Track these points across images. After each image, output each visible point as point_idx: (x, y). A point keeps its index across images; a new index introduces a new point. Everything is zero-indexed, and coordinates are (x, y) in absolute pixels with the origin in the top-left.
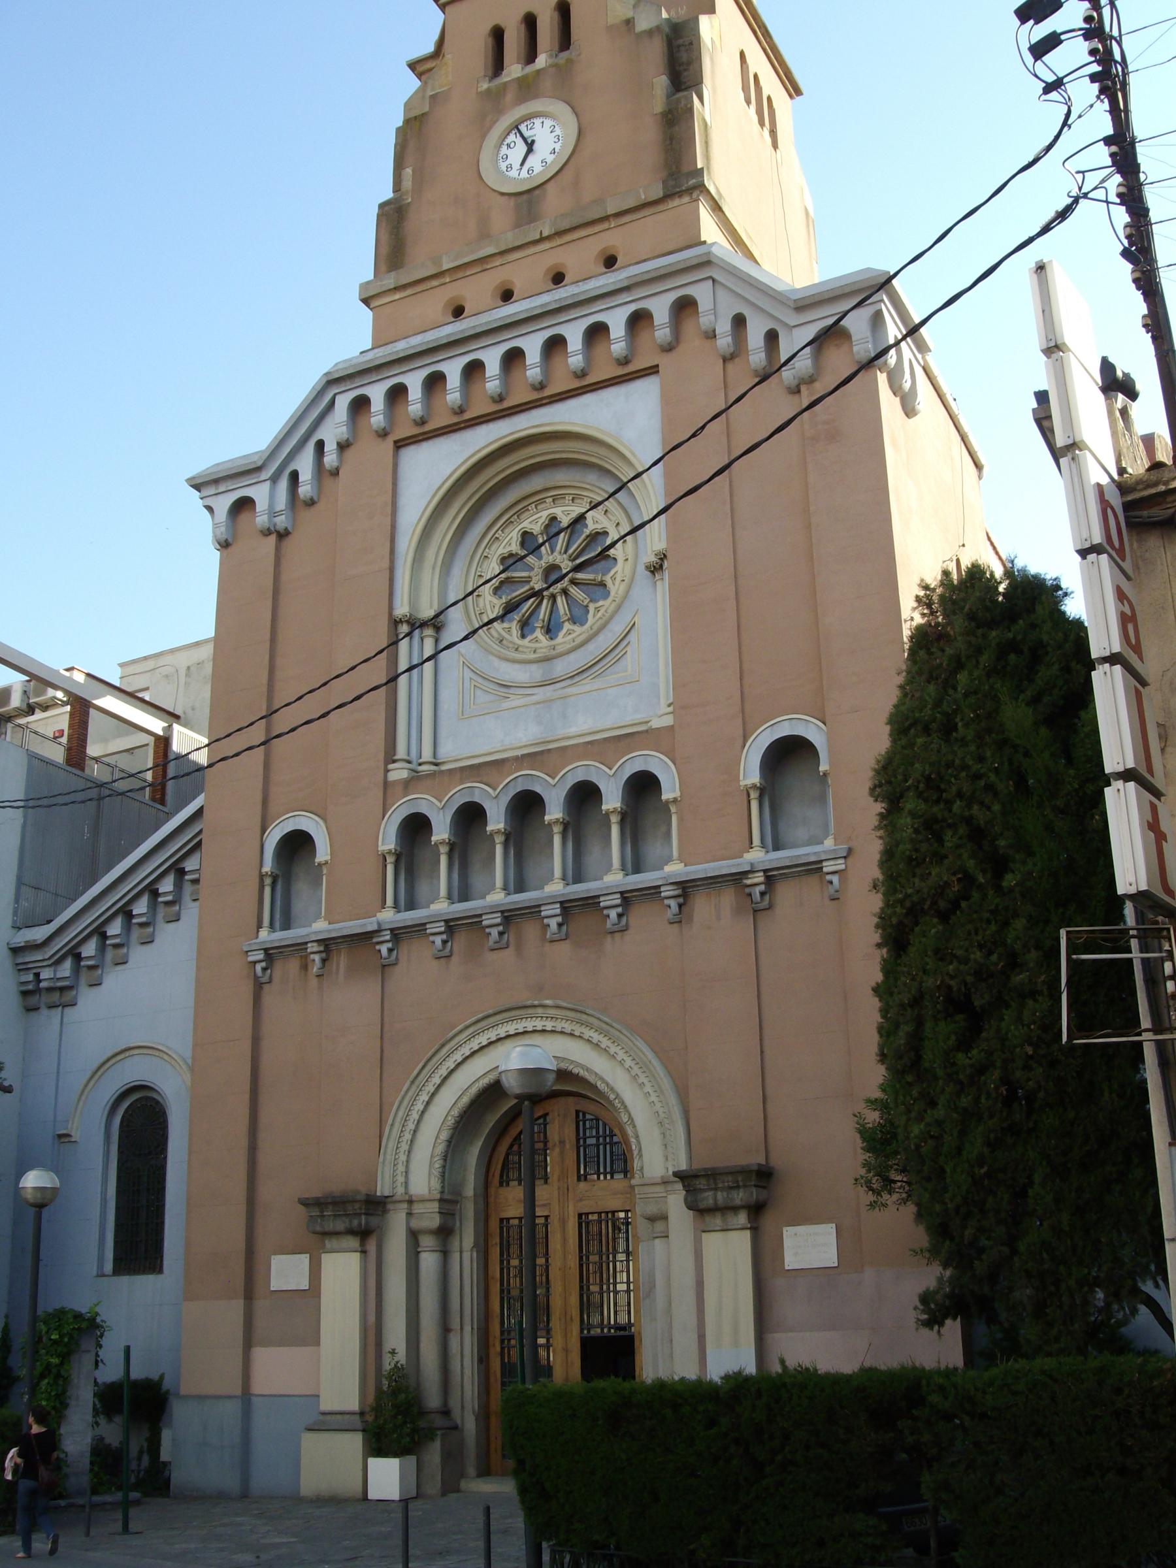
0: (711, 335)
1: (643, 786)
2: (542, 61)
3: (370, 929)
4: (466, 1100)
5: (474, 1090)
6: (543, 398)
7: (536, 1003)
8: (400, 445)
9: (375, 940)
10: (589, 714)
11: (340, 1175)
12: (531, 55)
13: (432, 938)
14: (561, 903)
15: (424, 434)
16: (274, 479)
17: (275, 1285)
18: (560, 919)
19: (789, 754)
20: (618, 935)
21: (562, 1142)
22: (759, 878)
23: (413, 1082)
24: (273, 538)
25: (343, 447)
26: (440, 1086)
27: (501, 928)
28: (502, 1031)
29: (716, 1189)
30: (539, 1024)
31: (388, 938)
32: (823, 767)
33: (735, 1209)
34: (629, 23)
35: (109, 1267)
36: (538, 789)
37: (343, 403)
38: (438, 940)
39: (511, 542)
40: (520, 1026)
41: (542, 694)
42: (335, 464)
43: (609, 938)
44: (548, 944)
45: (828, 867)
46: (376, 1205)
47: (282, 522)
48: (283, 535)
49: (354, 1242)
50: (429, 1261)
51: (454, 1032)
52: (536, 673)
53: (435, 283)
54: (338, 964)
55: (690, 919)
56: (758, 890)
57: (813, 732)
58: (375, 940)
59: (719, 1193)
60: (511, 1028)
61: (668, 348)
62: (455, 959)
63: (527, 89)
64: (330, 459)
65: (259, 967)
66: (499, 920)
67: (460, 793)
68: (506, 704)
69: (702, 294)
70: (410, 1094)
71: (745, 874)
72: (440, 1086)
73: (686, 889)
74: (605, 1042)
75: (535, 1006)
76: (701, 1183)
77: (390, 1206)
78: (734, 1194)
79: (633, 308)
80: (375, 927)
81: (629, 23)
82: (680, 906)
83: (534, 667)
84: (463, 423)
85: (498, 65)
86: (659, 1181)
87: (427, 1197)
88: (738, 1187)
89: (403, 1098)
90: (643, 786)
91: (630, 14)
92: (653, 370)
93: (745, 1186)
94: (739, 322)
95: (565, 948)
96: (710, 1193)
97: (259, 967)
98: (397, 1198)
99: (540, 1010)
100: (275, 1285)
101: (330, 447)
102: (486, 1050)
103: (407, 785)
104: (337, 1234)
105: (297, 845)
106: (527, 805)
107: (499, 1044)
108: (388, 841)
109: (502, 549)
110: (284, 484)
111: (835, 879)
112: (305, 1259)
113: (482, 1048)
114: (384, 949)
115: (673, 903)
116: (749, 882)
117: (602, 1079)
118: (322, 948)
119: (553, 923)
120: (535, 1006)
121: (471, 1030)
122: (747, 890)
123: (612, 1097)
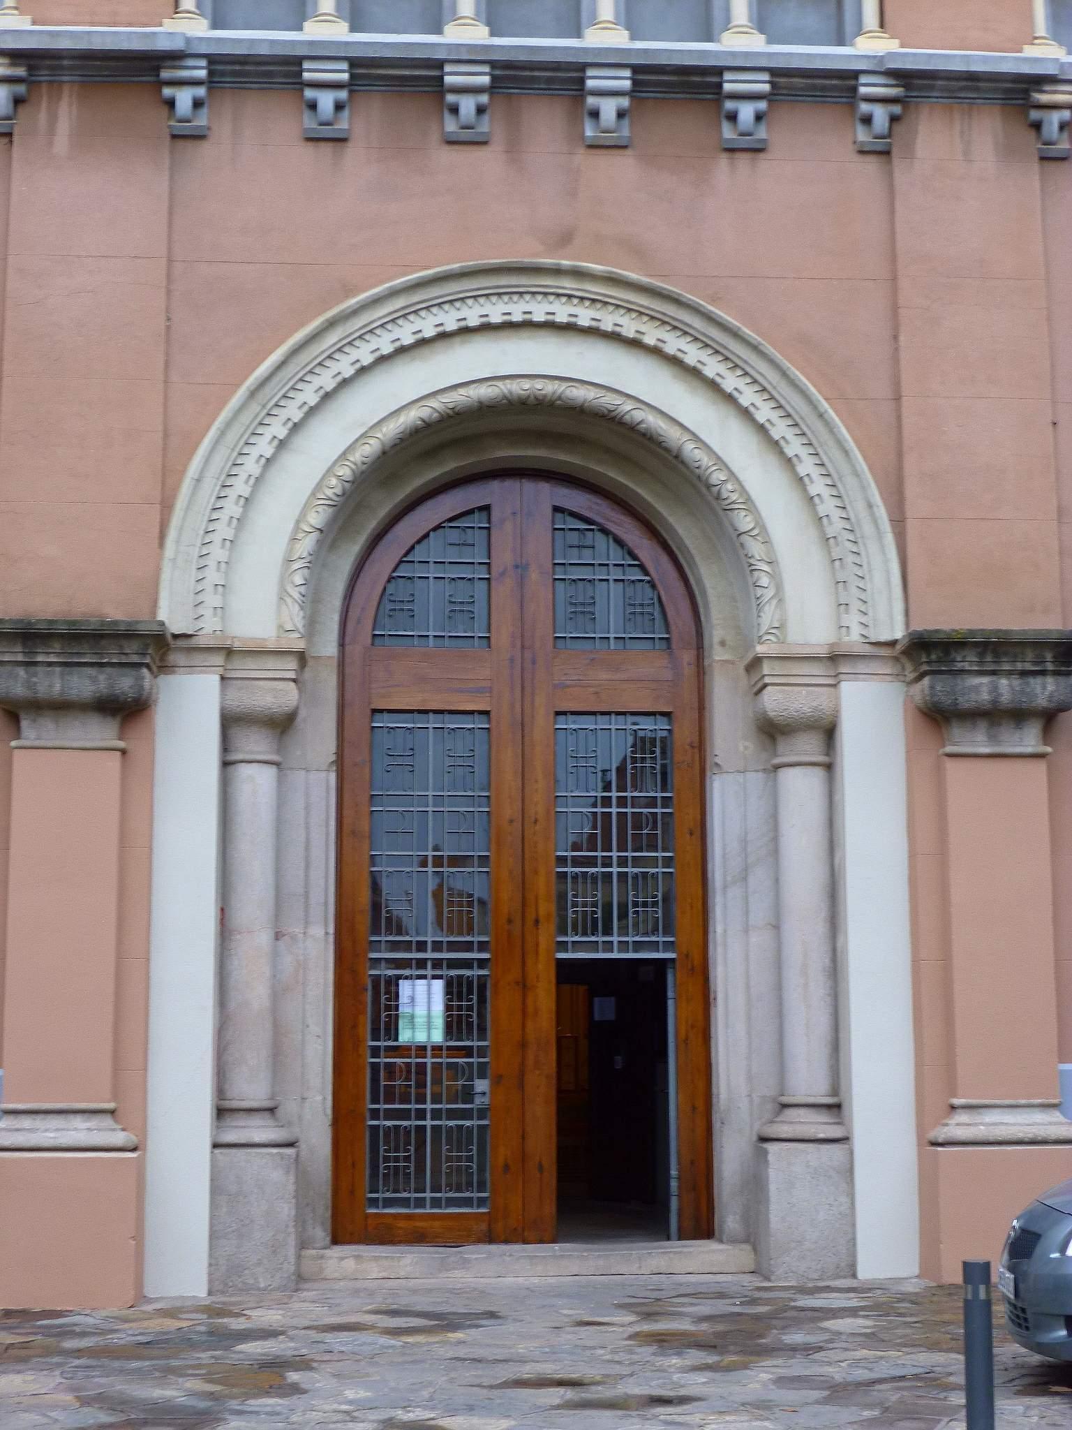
3: (163, 45)
4: (370, 449)
5: (392, 430)
7: (566, 263)
9: (165, 74)
13: (309, 93)
14: (636, 69)
18: (625, 102)
20: (738, 155)
21: (521, 568)
23: (253, 394)
26: (312, 411)
27: (484, 99)
28: (473, 314)
29: (994, 673)
30: (562, 312)
31: (202, 73)
33: (1018, 715)
38: (326, 100)
40: (517, 310)
43: (723, 161)
44: (582, 150)
46: (158, 648)
49: (101, 731)
50: (256, 783)
51: (353, 302)
54: (53, 120)
55: (910, 154)
56: (1055, 118)
58: (165, 74)
59: (1004, 682)
60: (495, 312)
62: (354, 154)
66: (486, 80)
70: (246, 417)
72: (312, 411)
73: (913, 85)
74: (713, 367)
75: (557, 272)
76: (967, 661)
78: (1036, 683)
80: (178, 45)
82: (894, 119)
86: (823, 651)
87: (271, 646)
88: (1043, 673)
89: (228, 425)
93: (1056, 673)
95: (623, 167)
96: (985, 680)
98: (201, 641)
99: (568, 284)
102: (425, 350)
104: (61, 707)
107: (439, 346)
113: (423, 343)
114: (184, 98)
115: (880, 114)
116: (1044, 98)
117: (696, 438)
118: (21, 72)
119: (608, 108)
120: (557, 272)
121: (400, 302)
122: (1034, 115)
123: (717, 477)
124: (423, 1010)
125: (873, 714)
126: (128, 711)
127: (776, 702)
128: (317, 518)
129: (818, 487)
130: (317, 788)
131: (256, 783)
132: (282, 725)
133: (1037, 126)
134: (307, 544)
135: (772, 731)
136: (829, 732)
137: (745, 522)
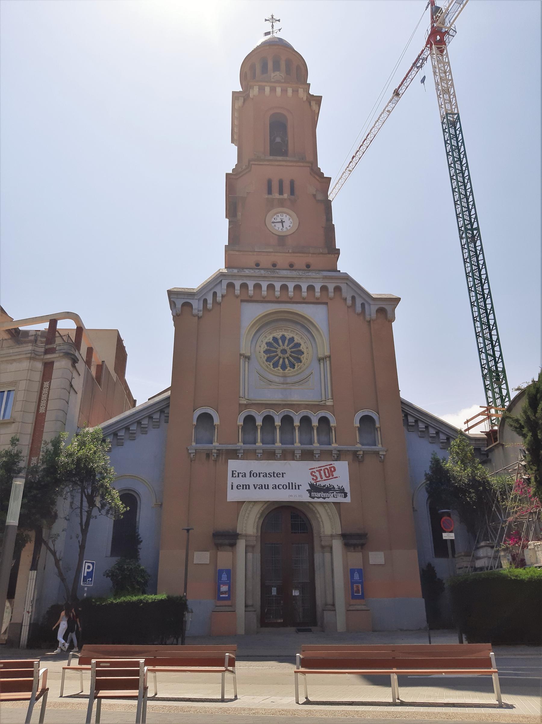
0: (345, 299)
1: (324, 421)
2: (285, 196)
6: (291, 301)
8: (242, 301)
10: (297, 396)
11: (223, 525)
12: (281, 192)
15: (250, 300)
16: (199, 300)
17: (195, 562)
19: (366, 420)
22: (361, 453)
24: (197, 318)
25: (223, 296)
32: (377, 425)
34: (314, 196)
35: (109, 554)
36: (291, 415)
37: (225, 283)
39: (270, 338)
41: (282, 386)
42: (221, 301)
45: (381, 453)
47: (201, 314)
48: (199, 318)
50: (250, 555)
52: (281, 380)
53: (250, 253)
57: (375, 416)
61: (331, 299)
63: (281, 203)
64: (219, 299)
65: (192, 455)
67: (266, 412)
68: (270, 387)
69: (344, 287)
71: (357, 451)
77: (239, 537)
79: (323, 284)
81: (314, 196)
83: (280, 378)
84: (264, 301)
85: (270, 192)
90: (324, 421)
91: (315, 193)
92: (326, 303)
94: (353, 298)
97: (192, 455)
100: (195, 562)
101: (219, 295)
103: (247, 406)
105: (206, 418)
106: (287, 420)
108: (241, 422)
109: (267, 340)
110: (201, 302)
111: (382, 457)
112: (207, 555)
124: (274, 591)
125: (337, 545)
126: (233, 545)
127: (323, 543)
128: (258, 516)
129: (329, 511)
130: (258, 556)
131: (250, 555)
132: (253, 547)
133: (358, 457)
134: (257, 520)
135: (323, 547)
136: (331, 548)
137: (318, 516)
